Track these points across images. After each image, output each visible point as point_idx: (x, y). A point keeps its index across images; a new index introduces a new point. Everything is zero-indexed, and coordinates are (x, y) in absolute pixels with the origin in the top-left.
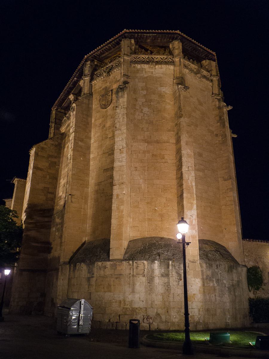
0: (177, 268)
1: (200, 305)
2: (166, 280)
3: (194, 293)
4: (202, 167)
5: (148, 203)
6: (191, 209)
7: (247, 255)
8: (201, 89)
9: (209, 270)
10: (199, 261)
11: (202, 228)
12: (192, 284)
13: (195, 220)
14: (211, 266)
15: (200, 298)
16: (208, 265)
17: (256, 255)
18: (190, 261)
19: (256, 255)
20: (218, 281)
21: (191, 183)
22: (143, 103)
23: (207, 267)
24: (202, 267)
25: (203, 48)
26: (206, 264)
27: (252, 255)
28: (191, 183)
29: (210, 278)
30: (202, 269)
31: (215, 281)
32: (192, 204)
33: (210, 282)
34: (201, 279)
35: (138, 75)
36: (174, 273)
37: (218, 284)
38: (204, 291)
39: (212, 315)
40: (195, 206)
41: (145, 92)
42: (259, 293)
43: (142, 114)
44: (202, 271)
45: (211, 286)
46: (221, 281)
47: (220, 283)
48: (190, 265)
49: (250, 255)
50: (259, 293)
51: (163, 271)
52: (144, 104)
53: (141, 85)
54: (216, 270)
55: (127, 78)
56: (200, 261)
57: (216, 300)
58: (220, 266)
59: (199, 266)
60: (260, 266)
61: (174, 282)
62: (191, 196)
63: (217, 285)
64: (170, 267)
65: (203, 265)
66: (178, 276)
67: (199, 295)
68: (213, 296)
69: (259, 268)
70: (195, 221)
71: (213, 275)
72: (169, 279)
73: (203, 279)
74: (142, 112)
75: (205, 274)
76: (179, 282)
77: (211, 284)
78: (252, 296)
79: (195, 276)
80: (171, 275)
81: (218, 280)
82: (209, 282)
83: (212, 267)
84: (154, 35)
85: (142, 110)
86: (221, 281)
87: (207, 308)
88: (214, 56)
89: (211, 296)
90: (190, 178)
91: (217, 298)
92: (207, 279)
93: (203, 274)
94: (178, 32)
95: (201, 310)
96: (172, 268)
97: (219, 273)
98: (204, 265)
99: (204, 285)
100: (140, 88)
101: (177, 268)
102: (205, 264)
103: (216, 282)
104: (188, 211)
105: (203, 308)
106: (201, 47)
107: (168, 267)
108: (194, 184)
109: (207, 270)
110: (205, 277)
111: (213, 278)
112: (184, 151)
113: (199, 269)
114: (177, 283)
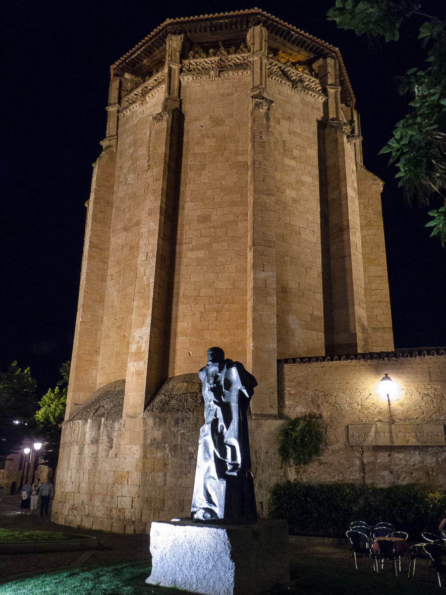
0: (109, 428)
1: (135, 490)
2: (94, 448)
3: (126, 470)
4: (207, 240)
5: (118, 327)
6: (142, 324)
9: (159, 430)
10: (142, 414)
11: (191, 353)
12: (126, 454)
13: (146, 342)
14: (163, 421)
15: (137, 478)
16: (157, 419)
17: (316, 390)
18: (128, 416)
19: (316, 390)
20: (174, 448)
21: (148, 279)
23: (155, 424)
24: (145, 423)
25: (227, 17)
26: (154, 419)
27: (307, 391)
28: (148, 279)
29: (158, 443)
30: (145, 429)
31: (168, 449)
32: (145, 315)
33: (157, 450)
34: (141, 445)
35: (127, 127)
38: (144, 467)
39: (155, 509)
41: (131, 151)
42: (315, 473)
43: (125, 188)
44: (145, 431)
47: (179, 451)
48: (127, 422)
49: (300, 392)
50: (315, 473)
51: (94, 435)
52: (130, 168)
53: (130, 139)
54: (174, 429)
55: (110, 140)
56: (143, 415)
57: (166, 484)
58: (183, 421)
59: (142, 424)
60: (325, 414)
62: (144, 303)
63: (171, 455)
64: (102, 428)
65: (148, 421)
66: (108, 442)
67: (135, 473)
69: (321, 416)
70: (146, 346)
71: (164, 437)
72: (98, 447)
74: (126, 184)
75: (149, 436)
76: (109, 451)
77: (159, 454)
78: (292, 476)
81: (175, 446)
82: (155, 450)
83: (165, 422)
84: (142, 49)
85: (127, 180)
86: (182, 448)
87: (146, 496)
88: (259, 13)
89: (157, 475)
91: (169, 479)
92: (151, 445)
93: (145, 438)
94: (168, 21)
95: (136, 499)
96: (104, 428)
98: (150, 421)
99: (145, 456)
101: (109, 428)
102: (152, 419)
103: (169, 450)
104: (137, 330)
105: (139, 497)
106: (222, 18)
107: (99, 428)
110: (149, 441)
111: (165, 443)
112: (144, 228)
113: (139, 428)
114: (106, 454)
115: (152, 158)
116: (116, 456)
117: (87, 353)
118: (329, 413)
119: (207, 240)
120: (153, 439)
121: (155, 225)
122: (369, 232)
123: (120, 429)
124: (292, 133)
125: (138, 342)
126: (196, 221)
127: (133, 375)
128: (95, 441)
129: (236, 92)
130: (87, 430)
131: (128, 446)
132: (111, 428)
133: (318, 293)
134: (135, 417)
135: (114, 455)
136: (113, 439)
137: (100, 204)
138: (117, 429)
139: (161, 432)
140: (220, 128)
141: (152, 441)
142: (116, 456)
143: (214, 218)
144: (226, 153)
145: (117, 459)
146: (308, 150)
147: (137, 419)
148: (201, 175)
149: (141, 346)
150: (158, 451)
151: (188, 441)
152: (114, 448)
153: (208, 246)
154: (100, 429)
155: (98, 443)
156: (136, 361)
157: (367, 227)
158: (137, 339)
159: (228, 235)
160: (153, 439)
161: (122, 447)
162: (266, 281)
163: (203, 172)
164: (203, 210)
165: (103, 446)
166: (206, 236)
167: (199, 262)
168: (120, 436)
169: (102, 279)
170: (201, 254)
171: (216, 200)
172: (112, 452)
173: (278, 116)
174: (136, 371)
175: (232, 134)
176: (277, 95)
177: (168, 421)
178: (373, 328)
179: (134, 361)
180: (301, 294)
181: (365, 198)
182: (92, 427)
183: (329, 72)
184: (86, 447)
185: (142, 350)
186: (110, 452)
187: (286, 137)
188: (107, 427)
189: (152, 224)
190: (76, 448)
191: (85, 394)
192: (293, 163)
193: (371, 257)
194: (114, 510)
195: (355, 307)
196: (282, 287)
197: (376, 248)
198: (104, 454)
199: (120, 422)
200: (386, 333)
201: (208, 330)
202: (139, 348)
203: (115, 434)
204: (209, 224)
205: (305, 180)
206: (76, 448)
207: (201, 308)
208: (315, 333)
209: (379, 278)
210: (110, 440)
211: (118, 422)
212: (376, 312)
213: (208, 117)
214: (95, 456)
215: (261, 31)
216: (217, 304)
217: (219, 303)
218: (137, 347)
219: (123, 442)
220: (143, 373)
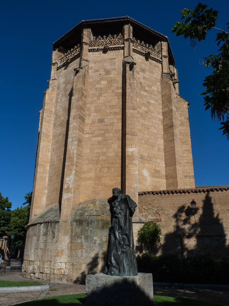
0: (53, 227)
2: (45, 237)
4: (103, 132)
7: (146, 209)
8: (111, 59)
9: (79, 228)
16: (78, 223)
18: (63, 221)
21: (73, 151)
22: (62, 94)
23: (77, 225)
24: (72, 225)
26: (76, 223)
28: (73, 151)
31: (83, 238)
32: (71, 170)
36: (51, 232)
37: (87, 240)
40: (74, 172)
44: (72, 229)
45: (78, 242)
46: (90, 238)
54: (87, 228)
58: (91, 224)
61: (50, 239)
64: (49, 228)
66: (52, 235)
68: (79, 251)
73: (72, 237)
76: (53, 239)
77: (79, 241)
79: (65, 234)
80: (49, 234)
81: (87, 237)
82: (77, 239)
83: (82, 225)
86: (90, 238)
90: (73, 148)
92: (75, 236)
93: (72, 232)
96: (50, 228)
97: (89, 230)
99: (71, 242)
100: (62, 84)
101: (53, 227)
103: (85, 238)
104: (67, 177)
108: (75, 152)
109: (76, 228)
110: (74, 234)
111: (82, 235)
114: (51, 241)
115: (75, 90)
116: (56, 242)
117: (41, 188)
118: (165, 219)
119: (103, 132)
120: (76, 233)
121: (77, 124)
122: (182, 128)
123: (58, 228)
124: (144, 78)
125: (68, 183)
126: (97, 122)
127: (65, 200)
128: (46, 234)
129: (117, 57)
130: (42, 228)
131: (63, 237)
132: (54, 227)
133: (158, 159)
134: (66, 222)
135: (55, 242)
136: (55, 233)
137: (48, 113)
138: (57, 228)
139: (80, 230)
140: (109, 76)
141: (75, 234)
142: (56, 242)
143: (106, 120)
144: (112, 88)
145: (57, 244)
146: (153, 87)
147: (68, 223)
148: (99, 99)
149: (70, 185)
150: (79, 239)
151: (94, 234)
152: (55, 238)
153: (102, 135)
154: (48, 228)
155: (47, 235)
156: (67, 193)
157: (182, 125)
158: (67, 182)
159: (113, 129)
160: (76, 233)
161: (60, 237)
162: (133, 152)
163: (101, 98)
164: (101, 117)
165: (50, 237)
166: (102, 130)
167: (99, 143)
168: (59, 231)
169: (48, 151)
170: (100, 139)
171: (107, 112)
172: (54, 240)
173: (138, 69)
174: (67, 198)
175: (115, 78)
176: (138, 60)
177: (83, 224)
178: (185, 176)
179: (66, 193)
180: (149, 159)
181: (180, 111)
182: (44, 227)
183: (163, 49)
184: (41, 237)
185: (70, 187)
186: (53, 240)
187: (142, 80)
188: (52, 227)
189: (75, 124)
190: (35, 238)
191: (40, 210)
192: (145, 94)
193: (184, 140)
194: (55, 270)
195: (177, 166)
196: (140, 155)
197: (186, 136)
198: (50, 241)
199: (59, 224)
200: (191, 178)
201: (103, 177)
202: (69, 186)
203: (56, 230)
204: (104, 124)
205: (151, 102)
206: (35, 238)
207: (100, 166)
208: (156, 179)
209: (187, 151)
210: (54, 233)
211: (58, 224)
212: (186, 168)
213: (103, 70)
214: (46, 242)
215: (129, 28)
216: (108, 164)
217: (109, 163)
218: (67, 186)
219: (60, 235)
220: (71, 199)
